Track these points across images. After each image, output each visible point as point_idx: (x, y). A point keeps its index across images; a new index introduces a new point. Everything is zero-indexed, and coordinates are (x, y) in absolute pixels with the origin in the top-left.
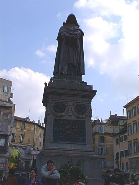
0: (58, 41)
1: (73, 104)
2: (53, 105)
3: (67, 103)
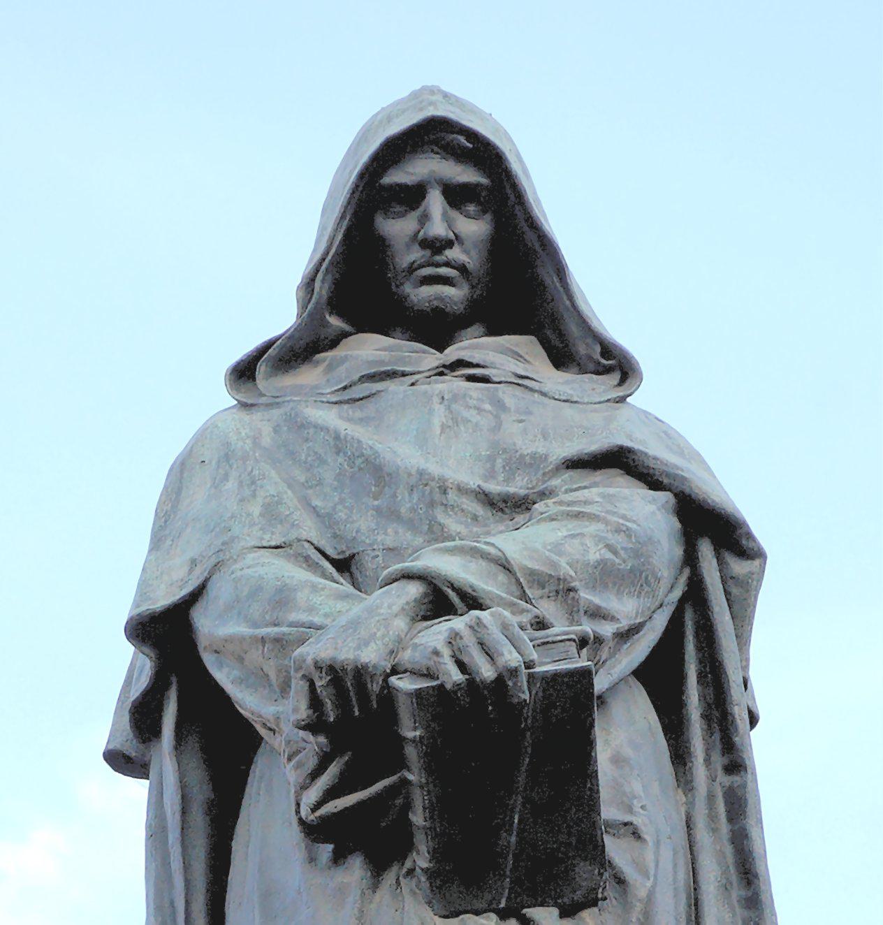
0: (138, 789)
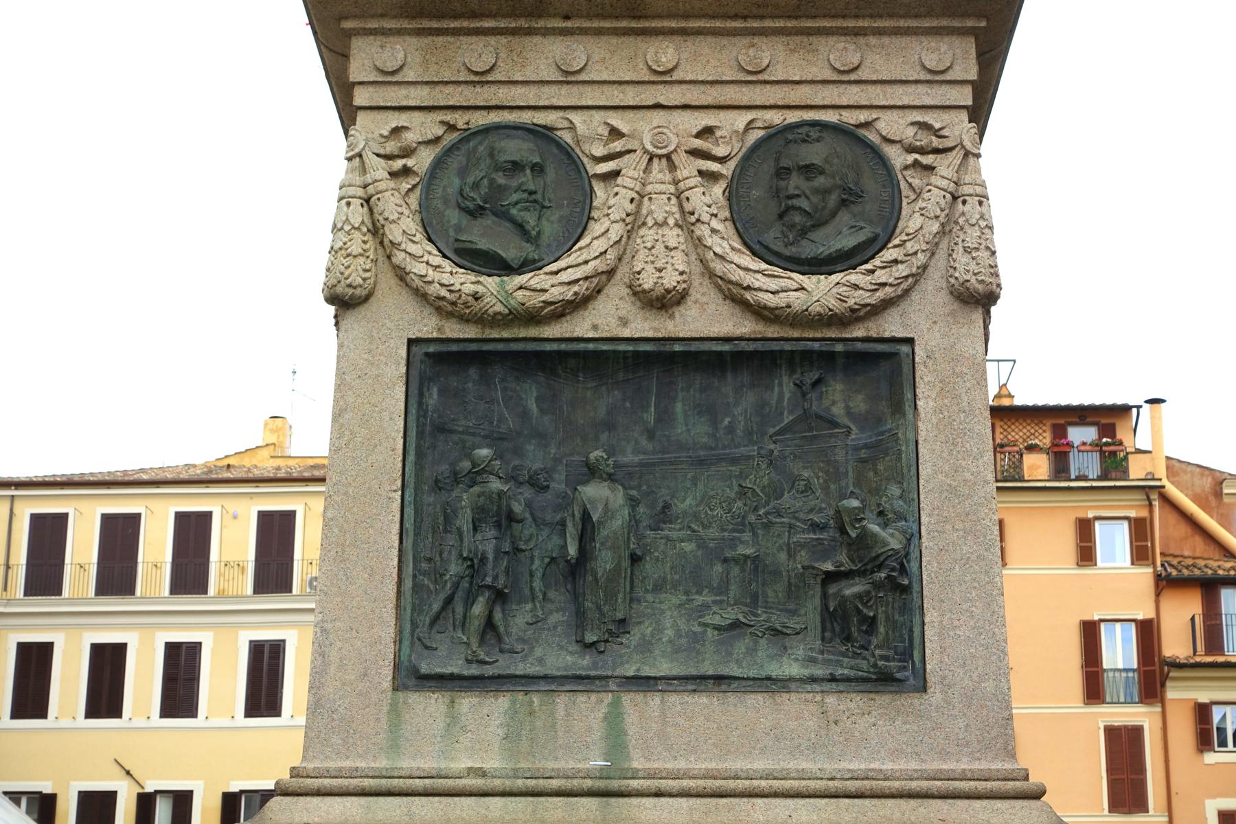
1: (707, 132)
2: (423, 161)
3: (615, 133)
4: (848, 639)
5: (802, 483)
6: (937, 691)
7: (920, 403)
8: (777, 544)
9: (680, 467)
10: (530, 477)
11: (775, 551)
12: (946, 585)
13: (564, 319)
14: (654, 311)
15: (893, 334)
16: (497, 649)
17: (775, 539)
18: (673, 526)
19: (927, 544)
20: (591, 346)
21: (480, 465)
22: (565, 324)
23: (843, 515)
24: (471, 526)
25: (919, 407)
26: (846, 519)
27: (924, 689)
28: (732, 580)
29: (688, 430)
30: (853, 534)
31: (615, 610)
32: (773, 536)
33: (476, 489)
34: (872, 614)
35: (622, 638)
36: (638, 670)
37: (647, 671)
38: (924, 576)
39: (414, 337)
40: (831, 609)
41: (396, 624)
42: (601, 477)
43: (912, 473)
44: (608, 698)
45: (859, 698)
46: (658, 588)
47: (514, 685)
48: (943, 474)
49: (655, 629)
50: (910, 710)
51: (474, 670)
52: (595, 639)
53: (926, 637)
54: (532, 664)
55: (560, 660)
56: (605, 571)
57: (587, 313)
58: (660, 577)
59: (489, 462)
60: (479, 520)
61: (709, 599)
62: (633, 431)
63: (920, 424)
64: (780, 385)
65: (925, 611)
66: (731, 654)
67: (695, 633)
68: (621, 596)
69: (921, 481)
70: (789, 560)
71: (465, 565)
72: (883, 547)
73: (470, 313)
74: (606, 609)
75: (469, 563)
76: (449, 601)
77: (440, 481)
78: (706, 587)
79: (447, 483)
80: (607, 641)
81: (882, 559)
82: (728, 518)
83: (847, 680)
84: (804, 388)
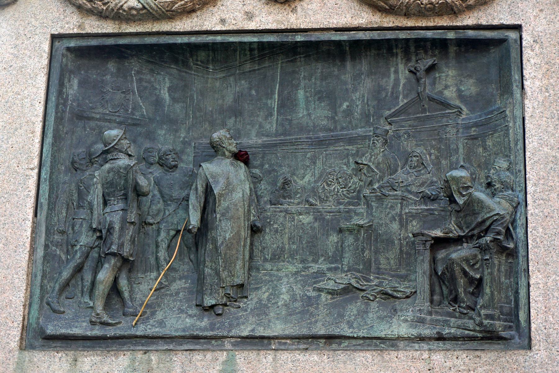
4: (456, 300)
5: (414, 159)
6: (541, 348)
7: (527, 83)
8: (390, 215)
9: (300, 147)
10: (160, 158)
11: (388, 222)
12: (551, 249)
13: (194, 15)
14: (278, 5)
15: (502, 22)
16: (121, 313)
17: (388, 210)
18: (292, 201)
19: (532, 211)
20: (219, 38)
21: (110, 144)
22: (196, 19)
23: (451, 184)
24: (101, 200)
25: (525, 87)
26: (454, 187)
27: (529, 347)
28: (347, 248)
29: (309, 115)
30: (461, 201)
31: (233, 276)
32: (386, 208)
33: (107, 166)
34: (478, 276)
35: (239, 302)
36: (253, 330)
37: (260, 332)
38: (529, 241)
39: (56, 33)
40: (439, 274)
41: (26, 290)
42: (224, 155)
43: (519, 147)
44: (223, 356)
45: (465, 355)
46: (276, 257)
47: (135, 345)
48: (549, 147)
49: (271, 294)
50: (515, 366)
51: (97, 331)
52: (214, 302)
53: (531, 297)
54: (153, 326)
55: (180, 322)
56: (225, 239)
57: (215, 9)
58: (278, 247)
59: (119, 140)
60: (109, 195)
61: (324, 267)
62: (258, 116)
63: (526, 102)
64: (396, 72)
65: (530, 273)
66: (341, 316)
67: (309, 298)
68: (239, 263)
69: (528, 154)
70: (401, 229)
71: (95, 237)
72: (489, 212)
73: (107, 9)
74: (224, 274)
75: (98, 234)
76: (79, 269)
77: (75, 162)
78: (322, 255)
79: (82, 164)
80: (225, 305)
81: (488, 223)
82: (345, 193)
83: (455, 338)
84: (418, 74)
